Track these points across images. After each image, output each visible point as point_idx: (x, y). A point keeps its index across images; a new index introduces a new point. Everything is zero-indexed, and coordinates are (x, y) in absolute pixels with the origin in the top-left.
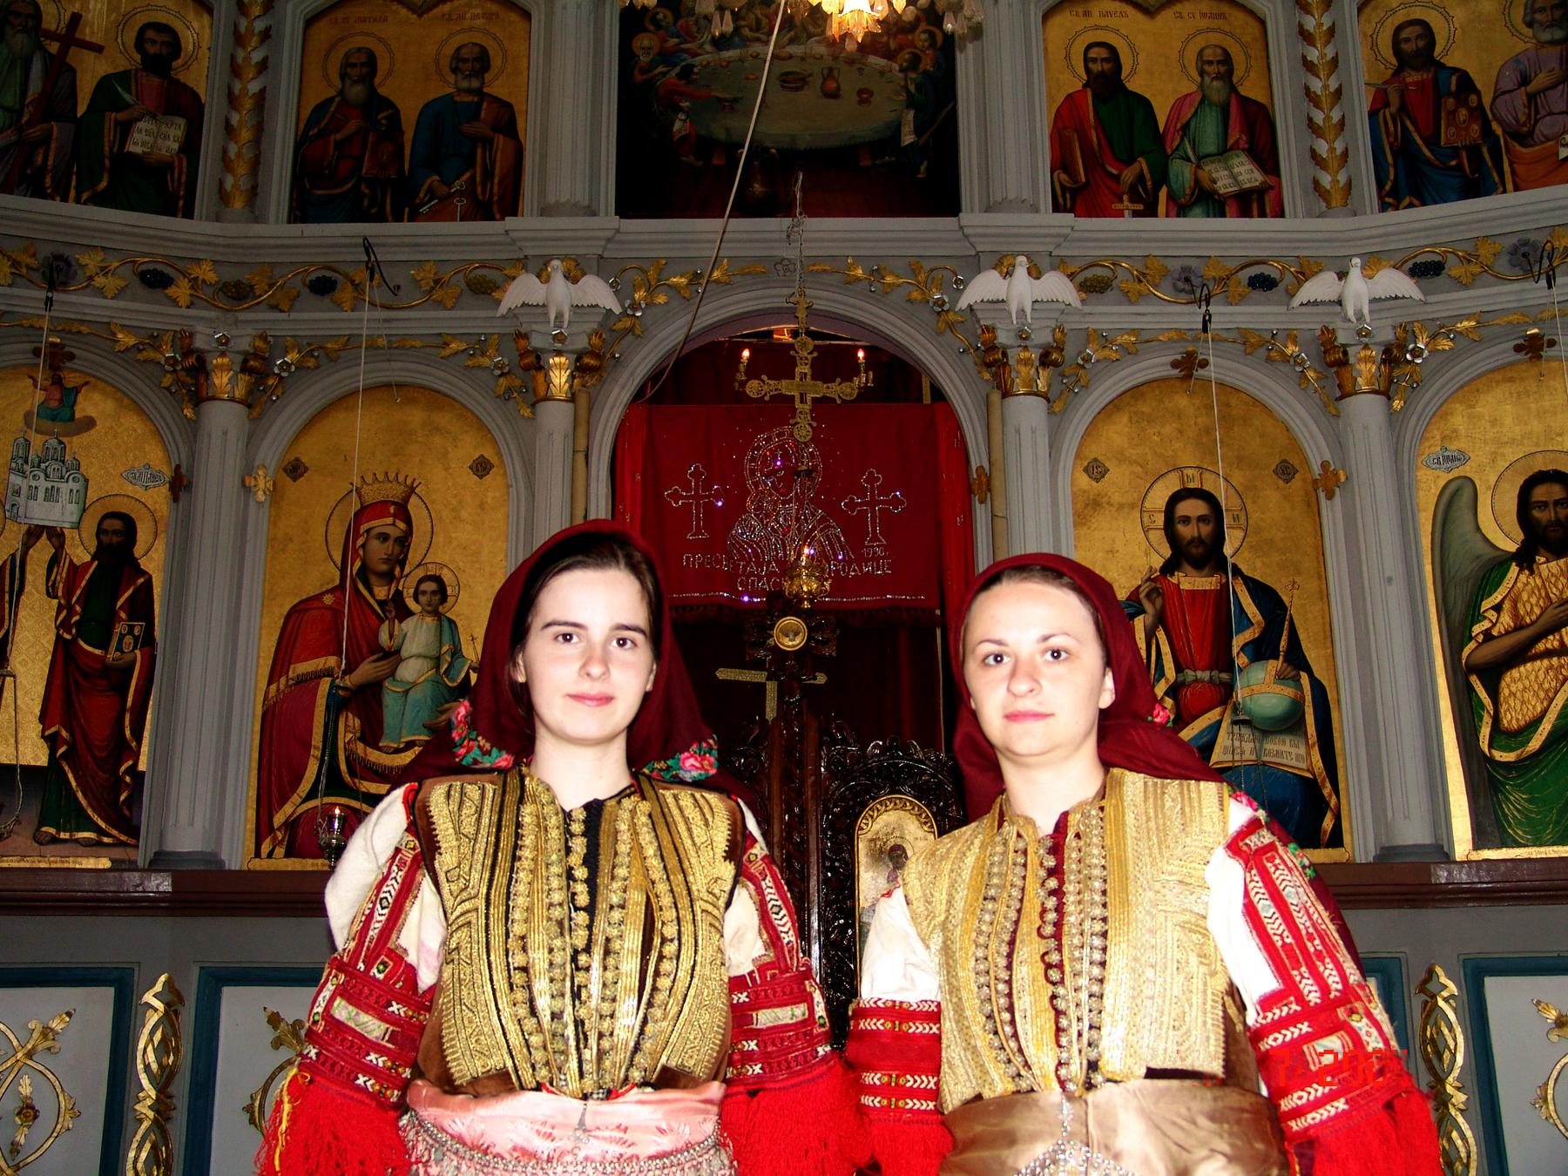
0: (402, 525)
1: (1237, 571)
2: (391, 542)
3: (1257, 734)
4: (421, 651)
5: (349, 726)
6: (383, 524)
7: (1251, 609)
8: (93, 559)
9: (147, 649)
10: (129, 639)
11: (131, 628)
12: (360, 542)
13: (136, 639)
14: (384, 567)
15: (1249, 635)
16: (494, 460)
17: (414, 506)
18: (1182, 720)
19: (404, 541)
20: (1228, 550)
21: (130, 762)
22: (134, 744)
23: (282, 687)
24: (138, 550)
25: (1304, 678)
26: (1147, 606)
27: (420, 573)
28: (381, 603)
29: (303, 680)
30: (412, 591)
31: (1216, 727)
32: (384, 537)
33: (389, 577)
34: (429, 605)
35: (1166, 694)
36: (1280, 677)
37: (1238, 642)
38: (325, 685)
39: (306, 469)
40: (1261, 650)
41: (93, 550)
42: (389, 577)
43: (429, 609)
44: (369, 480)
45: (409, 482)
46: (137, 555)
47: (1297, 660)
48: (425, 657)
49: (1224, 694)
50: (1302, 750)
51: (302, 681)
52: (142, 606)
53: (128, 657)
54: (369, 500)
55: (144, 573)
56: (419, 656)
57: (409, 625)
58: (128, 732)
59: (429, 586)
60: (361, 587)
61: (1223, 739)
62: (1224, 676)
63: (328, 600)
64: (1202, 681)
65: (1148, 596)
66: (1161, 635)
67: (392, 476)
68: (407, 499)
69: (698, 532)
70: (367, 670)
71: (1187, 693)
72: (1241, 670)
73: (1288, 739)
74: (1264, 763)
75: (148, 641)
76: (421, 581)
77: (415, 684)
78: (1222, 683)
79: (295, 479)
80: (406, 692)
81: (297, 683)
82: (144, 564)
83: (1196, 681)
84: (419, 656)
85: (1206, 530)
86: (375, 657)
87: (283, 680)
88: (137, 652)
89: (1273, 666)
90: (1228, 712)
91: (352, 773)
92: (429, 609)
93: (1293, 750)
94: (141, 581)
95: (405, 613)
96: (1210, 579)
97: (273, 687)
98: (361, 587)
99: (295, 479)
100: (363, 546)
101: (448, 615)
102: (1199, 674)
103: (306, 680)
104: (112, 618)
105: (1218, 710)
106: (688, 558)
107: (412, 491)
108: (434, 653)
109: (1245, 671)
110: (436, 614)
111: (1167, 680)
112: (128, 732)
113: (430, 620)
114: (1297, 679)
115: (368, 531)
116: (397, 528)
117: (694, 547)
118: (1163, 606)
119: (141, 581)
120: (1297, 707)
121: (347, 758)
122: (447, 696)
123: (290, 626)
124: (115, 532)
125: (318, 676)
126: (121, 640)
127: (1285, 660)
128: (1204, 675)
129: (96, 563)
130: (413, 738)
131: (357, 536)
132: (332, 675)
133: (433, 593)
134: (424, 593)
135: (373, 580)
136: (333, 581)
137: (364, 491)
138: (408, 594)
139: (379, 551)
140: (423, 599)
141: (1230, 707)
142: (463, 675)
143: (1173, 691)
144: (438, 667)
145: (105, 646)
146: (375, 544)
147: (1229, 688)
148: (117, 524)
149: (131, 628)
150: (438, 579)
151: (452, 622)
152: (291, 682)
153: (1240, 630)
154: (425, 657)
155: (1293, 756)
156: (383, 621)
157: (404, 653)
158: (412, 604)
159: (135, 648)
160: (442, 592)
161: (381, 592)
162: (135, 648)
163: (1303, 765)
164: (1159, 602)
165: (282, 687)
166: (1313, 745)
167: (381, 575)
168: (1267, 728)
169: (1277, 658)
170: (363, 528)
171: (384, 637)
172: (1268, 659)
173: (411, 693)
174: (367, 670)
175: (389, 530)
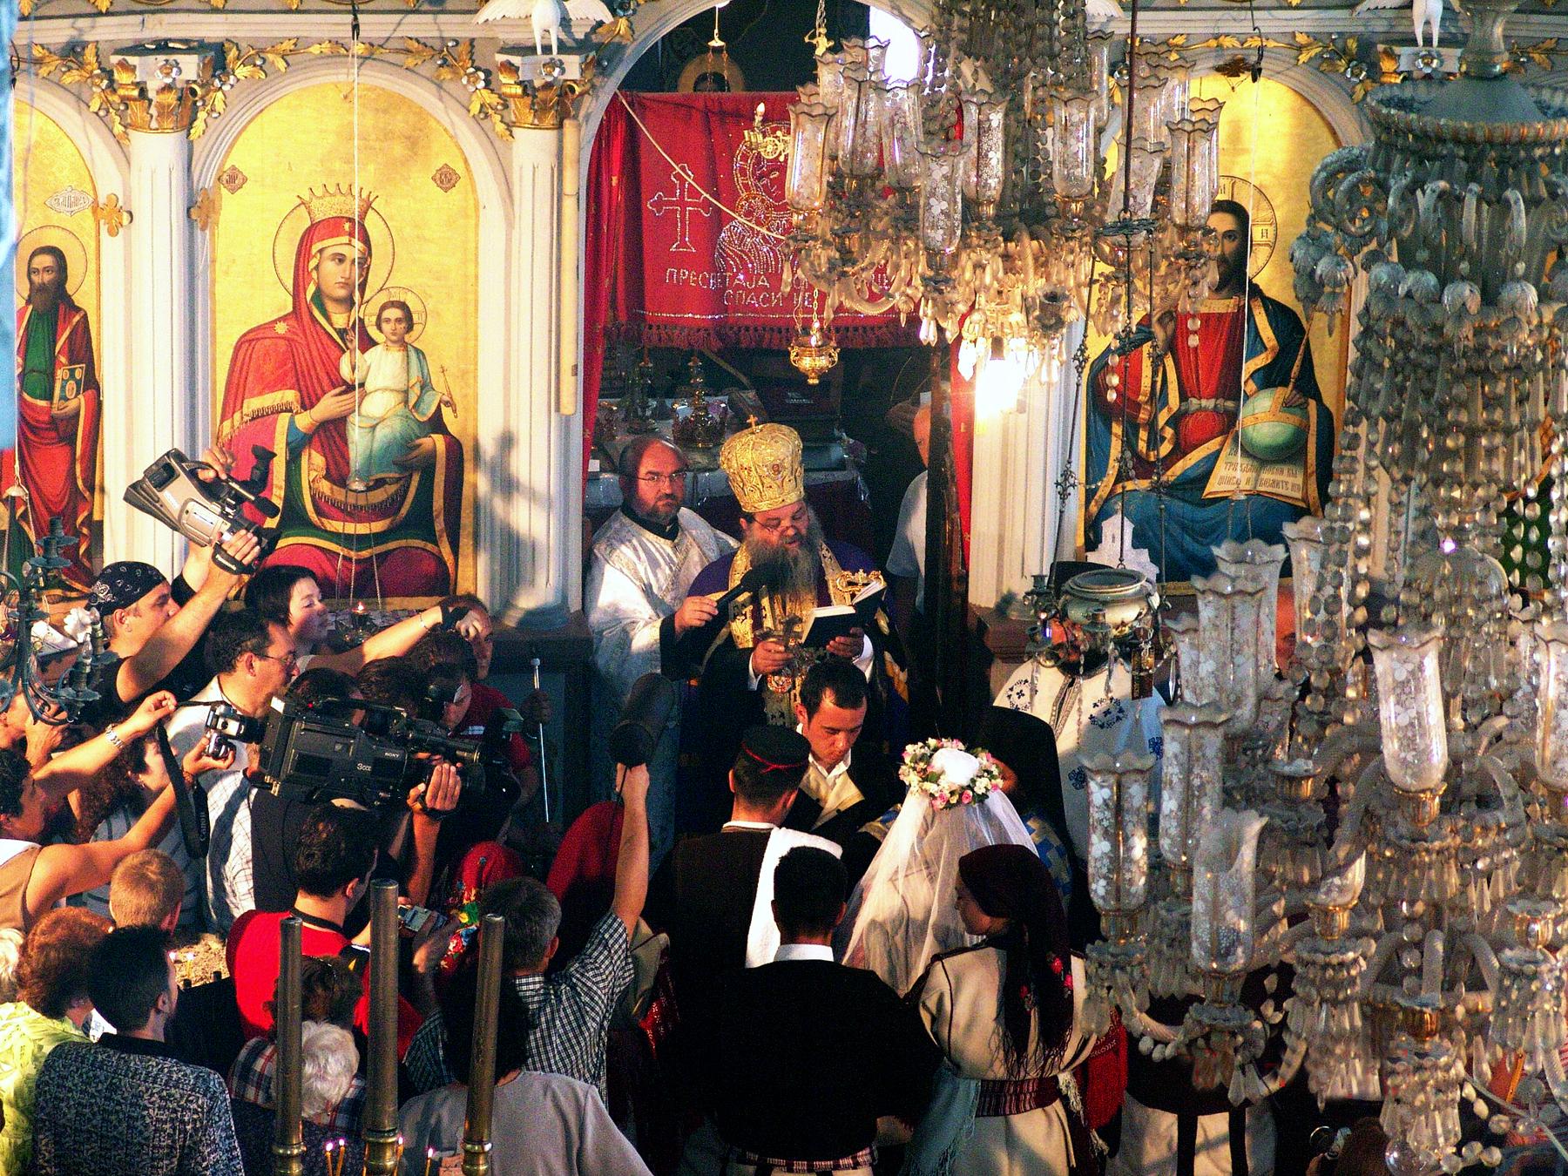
0: (358, 244)
1: (1256, 291)
2: (347, 264)
3: (1255, 463)
4: (390, 384)
5: (313, 463)
6: (335, 244)
7: (1267, 333)
8: (28, 302)
9: (90, 392)
10: (71, 384)
11: (72, 372)
12: (313, 264)
13: (78, 383)
14: (342, 293)
15: (1261, 361)
16: (459, 168)
17: (372, 223)
18: (1179, 451)
19: (364, 263)
20: (1250, 271)
21: (86, 514)
22: (87, 494)
23: (237, 424)
24: (70, 287)
25: (1312, 404)
26: (1157, 330)
27: (383, 298)
28: (342, 333)
29: (257, 416)
30: (374, 319)
31: (1216, 456)
32: (341, 259)
33: (349, 302)
34: (394, 334)
35: (1167, 423)
36: (1287, 405)
37: (1248, 367)
38: (284, 419)
39: (245, 180)
40: (1269, 378)
41: (26, 295)
42: (349, 302)
43: (394, 338)
44: (319, 192)
45: (364, 195)
46: (70, 293)
47: (1307, 386)
48: (392, 390)
49: (1227, 423)
50: (1299, 480)
51: (258, 417)
52: (83, 351)
53: (72, 404)
54: (319, 217)
55: (78, 309)
56: (385, 389)
57: (373, 353)
58: (80, 483)
59: (394, 313)
60: (317, 313)
61: (1220, 470)
62: (1230, 404)
63: (281, 328)
64: (1205, 409)
65: (1160, 320)
66: (1169, 362)
67: (344, 189)
68: (363, 215)
69: (683, 244)
70: (328, 406)
71: (1190, 422)
72: (1247, 397)
73: (1286, 468)
74: (1259, 494)
75: (91, 384)
76: (383, 308)
77: (383, 420)
78: (1226, 412)
79: (233, 191)
80: (373, 428)
81: (253, 419)
82: (79, 300)
83: (1200, 409)
84: (385, 389)
85: (1230, 246)
86: (337, 390)
87: (237, 416)
88: (81, 396)
89: (1282, 393)
90: (1229, 441)
91: (319, 512)
92: (394, 338)
93: (1291, 480)
94: (77, 318)
95: (367, 343)
96: (1227, 302)
97: (227, 424)
98: (317, 313)
99: (233, 191)
100: (317, 268)
101: (415, 345)
102: (1204, 402)
103: (263, 416)
104: (53, 362)
105: (1219, 439)
106: (672, 274)
107: (367, 206)
108: (402, 386)
109: (1251, 400)
110: (404, 345)
111: (1170, 410)
112: (80, 483)
113: (396, 355)
114: (1303, 407)
115: (321, 251)
116: (355, 249)
117: (682, 261)
118: (1175, 331)
119: (77, 318)
120: (1300, 435)
121: (313, 497)
122: (417, 431)
123: (240, 357)
124: (46, 269)
125: (277, 411)
126: (63, 387)
127: (1295, 387)
128: (1209, 404)
129: (30, 307)
130: (383, 475)
131: (309, 257)
132: (290, 411)
133: (398, 320)
134: (388, 320)
135: (330, 306)
136: (286, 308)
137: (315, 204)
138: (370, 322)
139: (332, 276)
140: (385, 326)
141: (1231, 436)
142: (433, 409)
143: (1176, 420)
144: (406, 402)
145: (49, 396)
146: (330, 267)
147: (1232, 417)
148: (46, 260)
149: (72, 372)
150: (403, 306)
151: (417, 350)
152: (246, 418)
153: (1253, 354)
154: (392, 390)
155: (1290, 486)
156: (344, 352)
157: (369, 387)
158: (373, 332)
159: (78, 393)
160: (408, 319)
161: (340, 320)
162: (78, 393)
163: (1298, 495)
164: (1171, 326)
165: (237, 424)
166: (1311, 475)
167: (337, 300)
168: (1264, 457)
169: (1285, 384)
170: (315, 249)
171: (345, 371)
172: (1276, 386)
173: (378, 428)
174: (328, 406)
175: (345, 250)
